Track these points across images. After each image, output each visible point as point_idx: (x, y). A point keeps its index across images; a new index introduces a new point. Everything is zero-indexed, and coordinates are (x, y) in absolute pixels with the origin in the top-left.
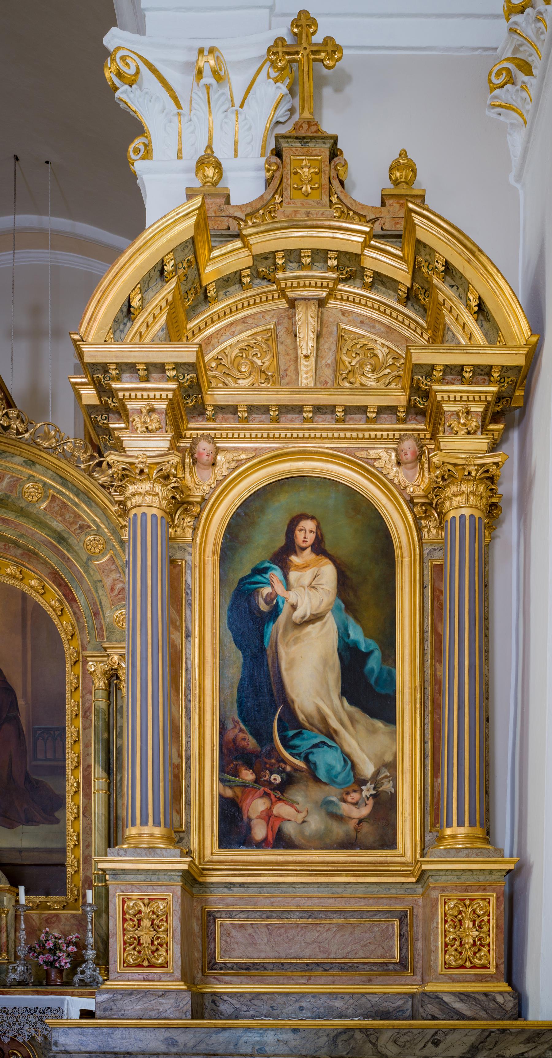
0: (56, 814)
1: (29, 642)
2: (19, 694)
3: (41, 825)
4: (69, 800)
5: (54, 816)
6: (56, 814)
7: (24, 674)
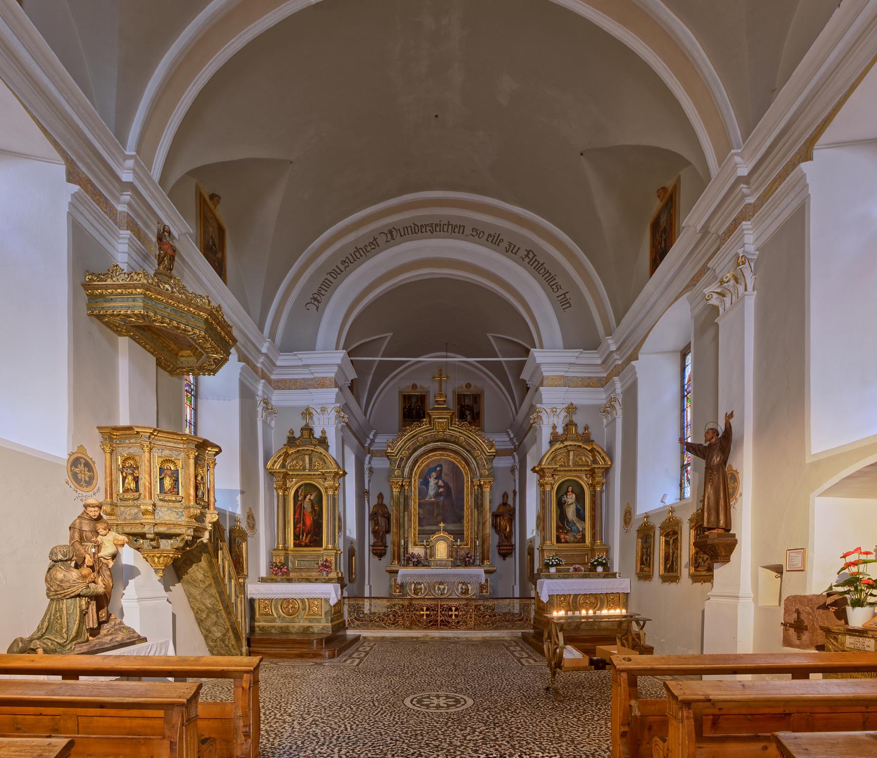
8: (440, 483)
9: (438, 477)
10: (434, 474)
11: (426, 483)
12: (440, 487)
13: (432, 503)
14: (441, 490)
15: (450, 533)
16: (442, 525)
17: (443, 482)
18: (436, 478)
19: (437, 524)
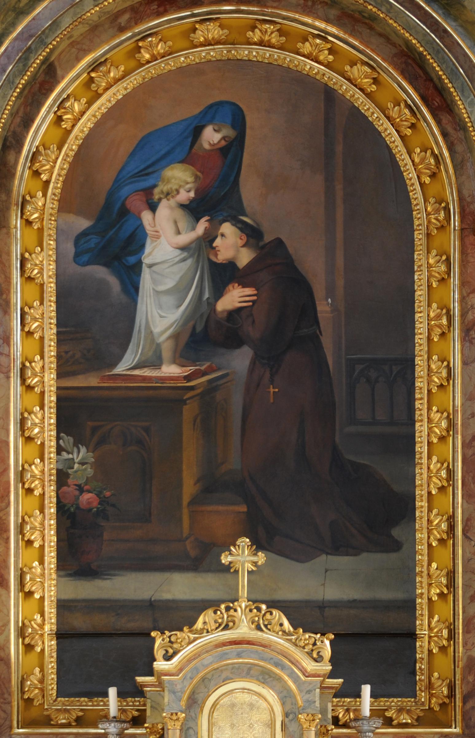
0: (396, 532)
1: (339, 188)
2: (319, 291)
3: (364, 555)
4: (421, 504)
5: (390, 536)
6: (396, 532)
7: (330, 250)
8: (230, 244)
9: (212, 203)
10: (180, 180)
11: (110, 241)
12: (223, 275)
13: (162, 402)
14: (235, 297)
15: (306, 616)
16: (243, 556)
17: (252, 234)
18: (194, 210)
19: (204, 558)
